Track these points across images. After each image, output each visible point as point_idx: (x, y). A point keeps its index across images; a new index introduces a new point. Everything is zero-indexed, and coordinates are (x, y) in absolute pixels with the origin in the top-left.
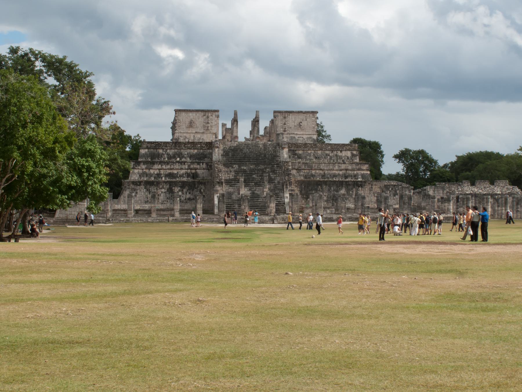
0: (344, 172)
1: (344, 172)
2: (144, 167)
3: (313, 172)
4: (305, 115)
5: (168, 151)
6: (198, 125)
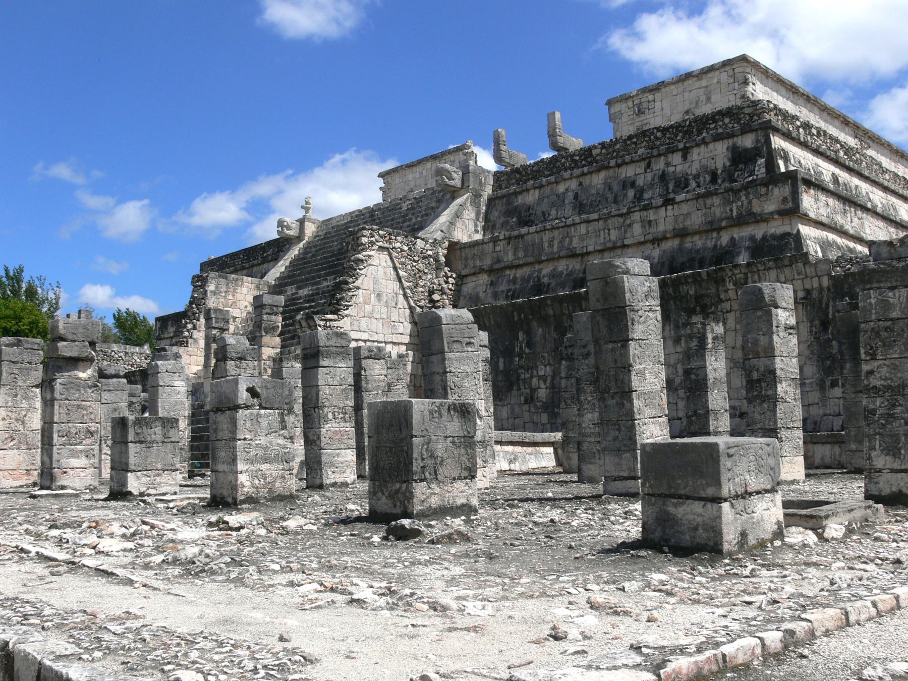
1: (668, 245)
3: (547, 269)
4: (704, 83)
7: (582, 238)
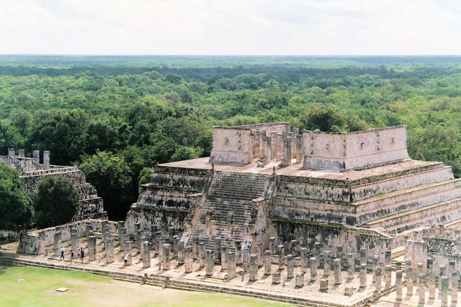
0: (329, 212)
2: (149, 192)
3: (299, 210)
5: (174, 176)
6: (231, 144)
7: (308, 205)
